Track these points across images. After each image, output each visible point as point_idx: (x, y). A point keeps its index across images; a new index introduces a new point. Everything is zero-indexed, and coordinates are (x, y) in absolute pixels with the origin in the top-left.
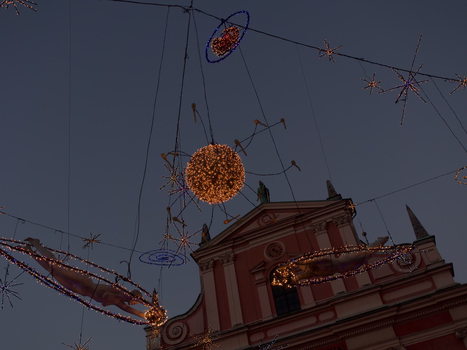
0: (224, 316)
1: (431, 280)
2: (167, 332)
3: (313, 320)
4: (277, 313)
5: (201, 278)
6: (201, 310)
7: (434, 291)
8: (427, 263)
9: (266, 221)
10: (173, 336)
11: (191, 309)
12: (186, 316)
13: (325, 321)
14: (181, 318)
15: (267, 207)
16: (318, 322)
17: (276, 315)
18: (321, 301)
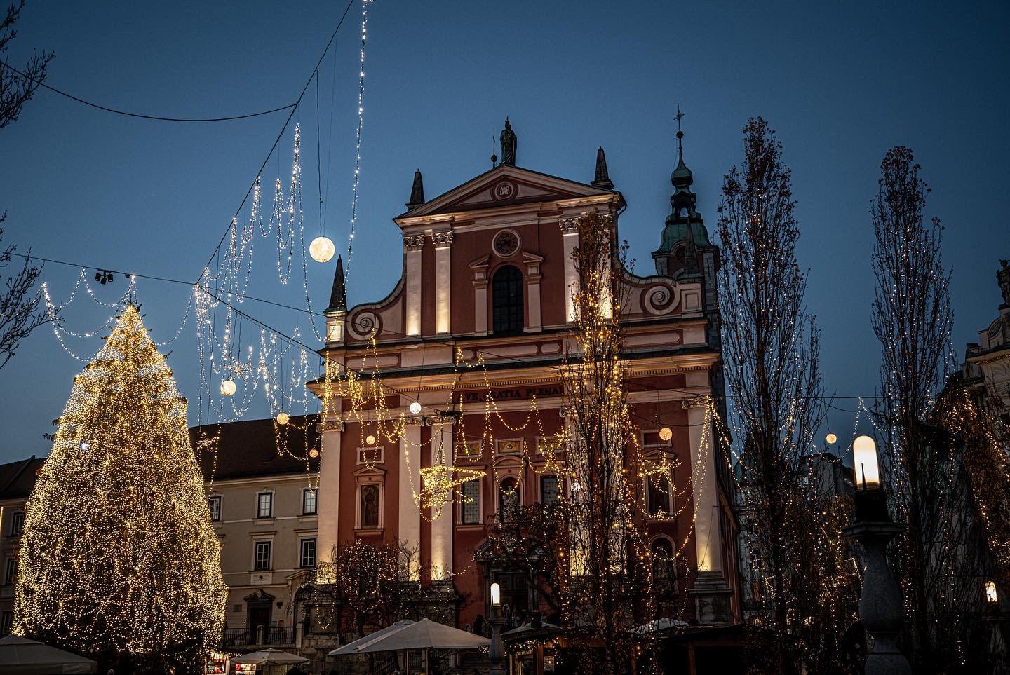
0: (428, 319)
1: (680, 333)
2: (353, 323)
3: (534, 350)
4: (494, 329)
5: (405, 256)
6: (400, 302)
7: (677, 347)
8: (684, 310)
9: (503, 193)
10: (361, 330)
11: (386, 299)
12: (379, 306)
13: (547, 354)
14: (373, 307)
15: (509, 171)
16: (539, 353)
17: (491, 333)
18: (547, 327)
